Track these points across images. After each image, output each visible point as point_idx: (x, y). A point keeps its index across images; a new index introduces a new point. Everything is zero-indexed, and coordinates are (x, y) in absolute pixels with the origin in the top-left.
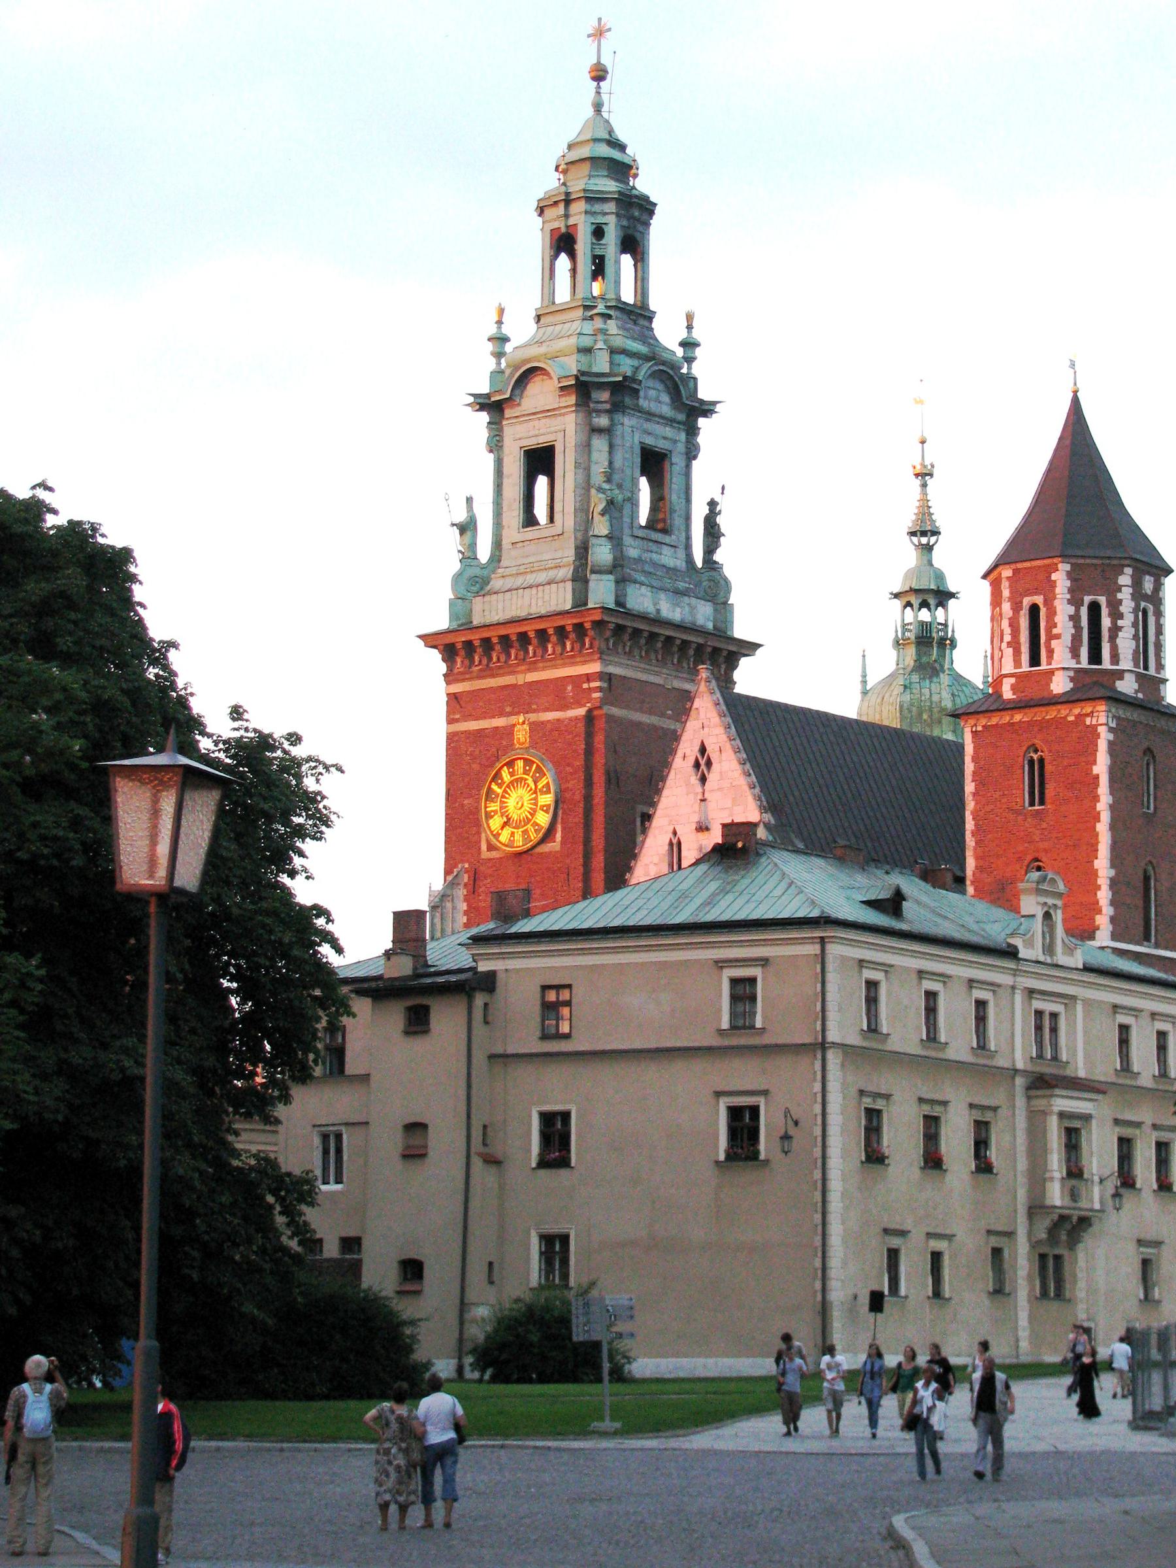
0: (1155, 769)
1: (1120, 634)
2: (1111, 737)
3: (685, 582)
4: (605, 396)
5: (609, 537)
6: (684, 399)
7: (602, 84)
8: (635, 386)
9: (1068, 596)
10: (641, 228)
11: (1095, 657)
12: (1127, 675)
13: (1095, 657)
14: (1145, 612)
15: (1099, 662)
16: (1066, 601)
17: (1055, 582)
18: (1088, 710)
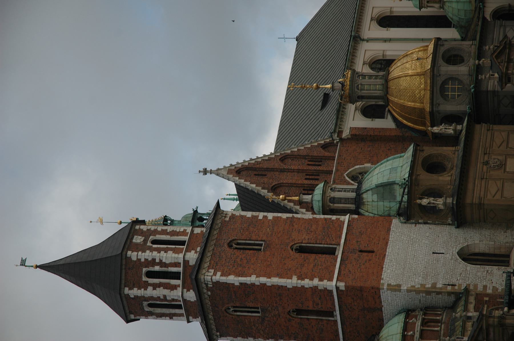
0: (240, 240)
1: (163, 261)
9: (143, 289)
11: (176, 276)
12: (186, 259)
13: (176, 276)
14: (154, 242)
16: (145, 291)
17: (134, 296)
18: (204, 286)
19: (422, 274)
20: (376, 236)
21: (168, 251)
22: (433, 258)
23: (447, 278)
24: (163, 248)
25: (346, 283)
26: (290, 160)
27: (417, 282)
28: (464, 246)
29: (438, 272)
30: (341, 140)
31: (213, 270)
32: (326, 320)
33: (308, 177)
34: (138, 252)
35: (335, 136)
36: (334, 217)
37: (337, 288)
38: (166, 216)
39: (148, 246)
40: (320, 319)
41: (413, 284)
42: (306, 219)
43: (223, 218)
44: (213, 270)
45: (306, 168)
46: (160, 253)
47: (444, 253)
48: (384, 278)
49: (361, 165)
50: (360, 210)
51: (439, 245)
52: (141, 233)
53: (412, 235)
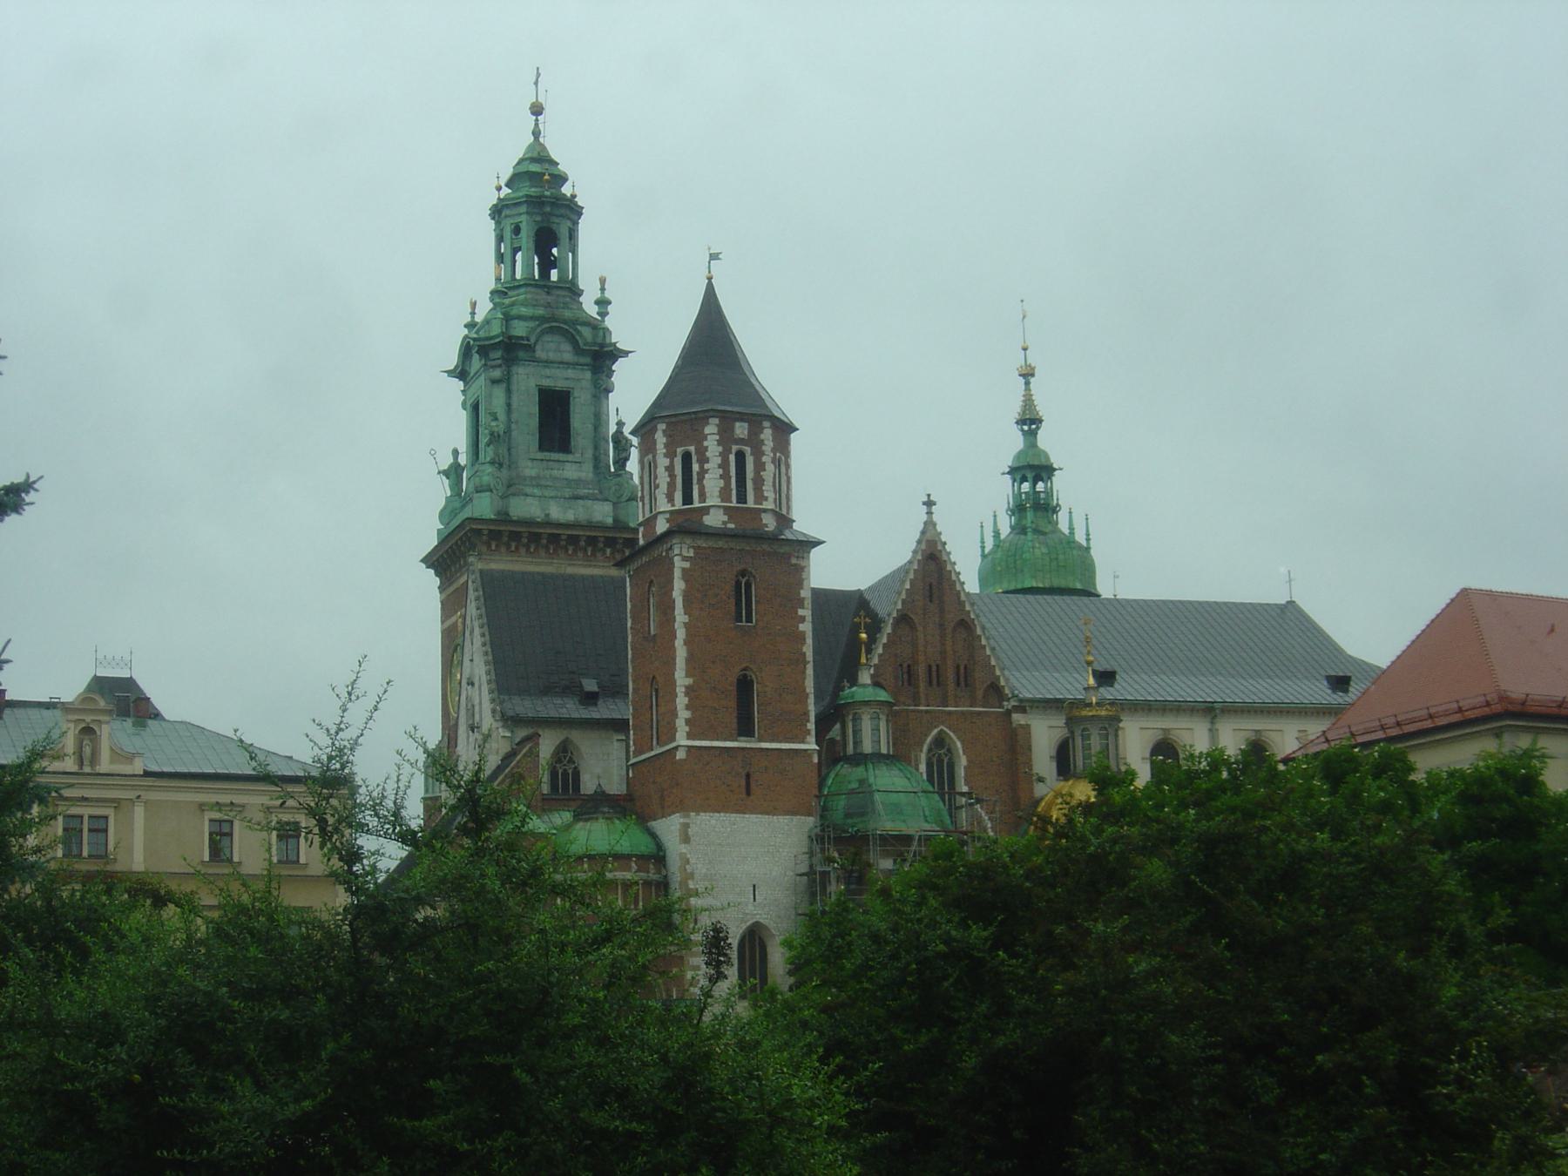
1: (706, 476)
2: (687, 565)
3: (589, 489)
4: (498, 354)
5: (492, 463)
6: (581, 345)
7: (539, 118)
8: (526, 342)
9: (664, 451)
10: (556, 220)
11: (688, 498)
12: (712, 511)
13: (688, 498)
14: (740, 457)
15: (692, 504)
18: (669, 546)
24: (729, 472)
25: (685, 760)
26: (964, 636)
27: (699, 867)
28: (773, 931)
30: (1008, 713)
31: (692, 555)
32: (652, 735)
33: (934, 668)
34: (718, 434)
35: (1013, 703)
36: (811, 726)
37: (676, 748)
38: (1041, 421)
39: (731, 448)
40: (652, 724)
41: (692, 861)
42: (804, 683)
43: (796, 554)
44: (692, 555)
45: (949, 662)
46: (720, 466)
47: (754, 899)
48: (699, 817)
49: (964, 750)
50: (841, 763)
51: (769, 892)
52: (755, 428)
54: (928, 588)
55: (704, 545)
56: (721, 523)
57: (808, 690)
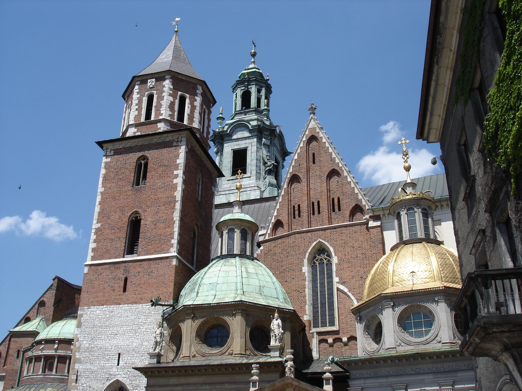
8: (225, 133)
10: (249, 87)
19: (92, 346)
20: (146, 290)
21: (138, 110)
22: (112, 354)
23: (86, 373)
24: (142, 106)
25: (87, 273)
26: (337, 180)
28: (128, 386)
29: (94, 363)
33: (316, 204)
36: (175, 241)
43: (177, 140)
46: (136, 105)
47: (118, 365)
48: (90, 309)
51: (129, 358)
53: (144, 327)
54: (311, 156)
55: (121, 147)
56: (132, 133)
57: (175, 219)
